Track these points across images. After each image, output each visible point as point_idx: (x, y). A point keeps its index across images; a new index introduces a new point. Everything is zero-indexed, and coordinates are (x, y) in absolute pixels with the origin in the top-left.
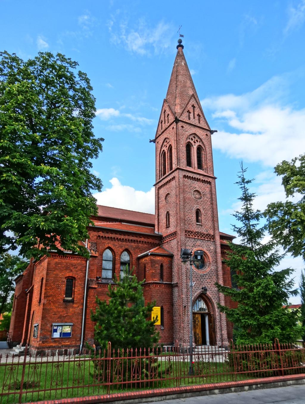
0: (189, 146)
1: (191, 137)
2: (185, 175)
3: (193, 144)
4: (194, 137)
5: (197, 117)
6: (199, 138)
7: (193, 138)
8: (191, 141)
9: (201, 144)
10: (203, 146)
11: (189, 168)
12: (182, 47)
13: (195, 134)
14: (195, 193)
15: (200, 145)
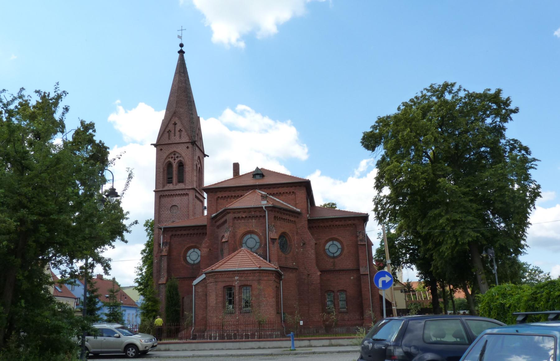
0: (170, 165)
1: (171, 156)
2: (161, 195)
3: (173, 162)
4: (175, 154)
5: (177, 133)
6: (179, 153)
7: (173, 156)
8: (170, 160)
9: (181, 159)
10: (183, 160)
11: (170, 187)
12: (184, 52)
13: (175, 151)
14: (174, 208)
15: (180, 160)
